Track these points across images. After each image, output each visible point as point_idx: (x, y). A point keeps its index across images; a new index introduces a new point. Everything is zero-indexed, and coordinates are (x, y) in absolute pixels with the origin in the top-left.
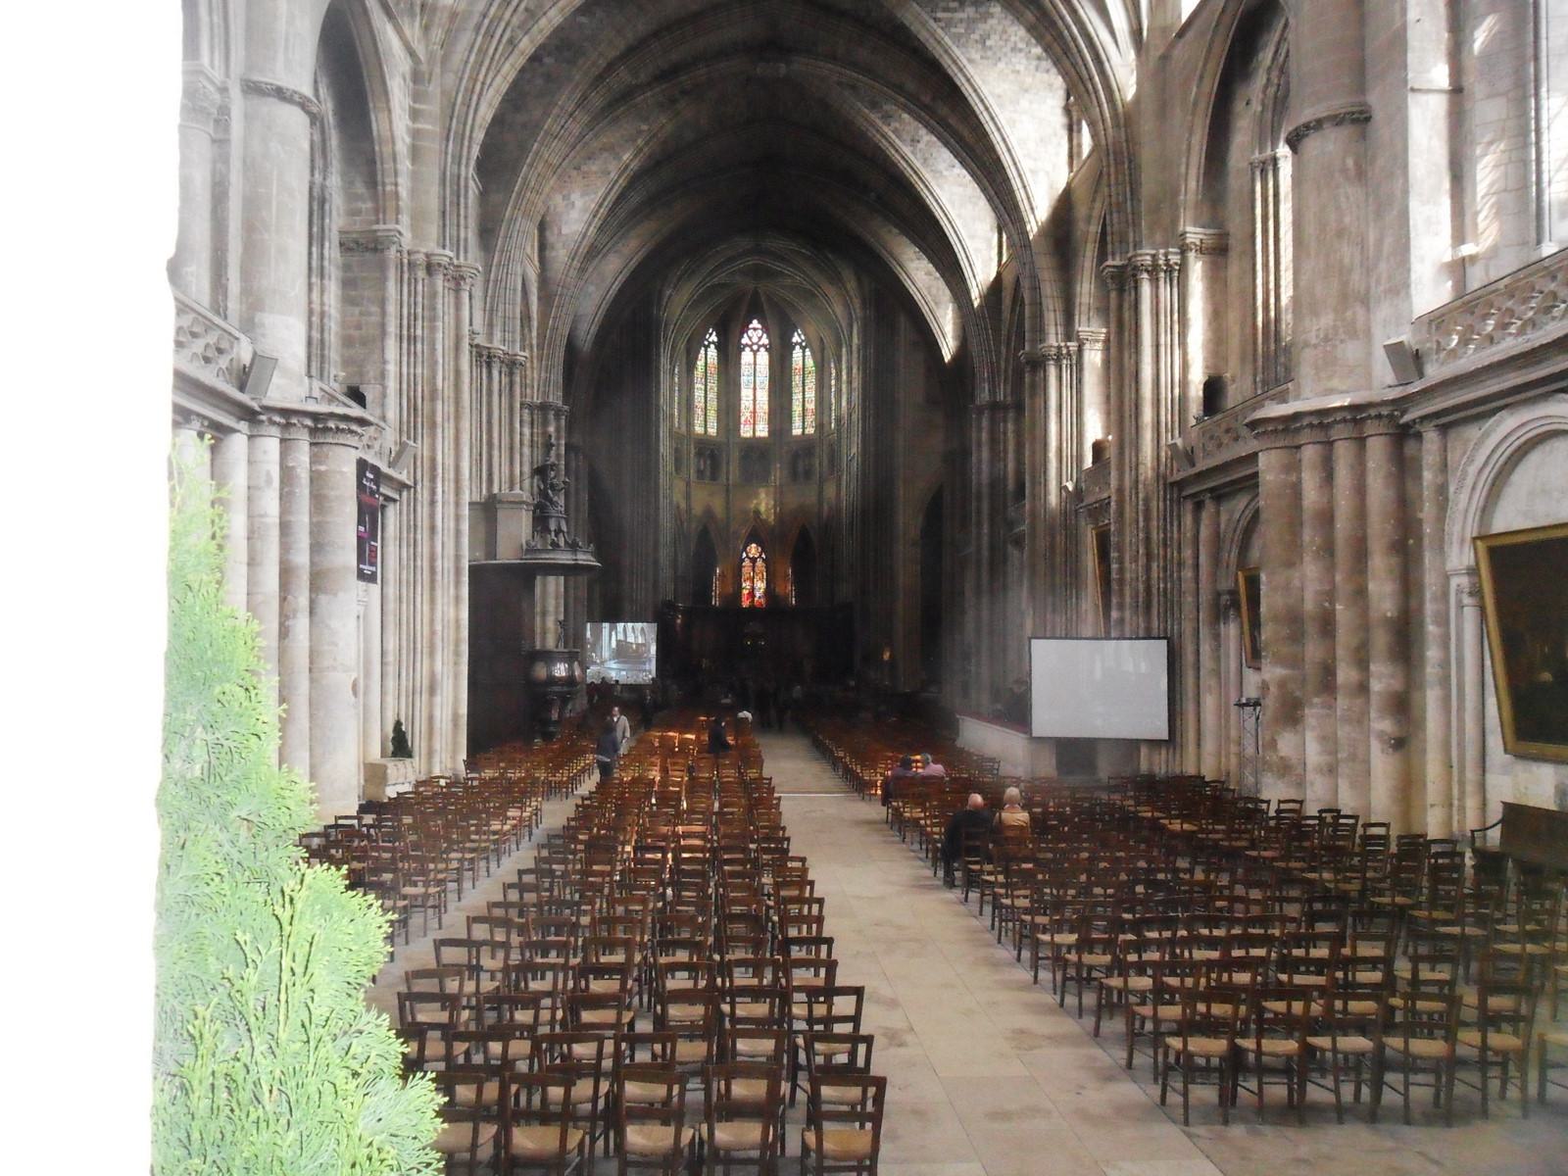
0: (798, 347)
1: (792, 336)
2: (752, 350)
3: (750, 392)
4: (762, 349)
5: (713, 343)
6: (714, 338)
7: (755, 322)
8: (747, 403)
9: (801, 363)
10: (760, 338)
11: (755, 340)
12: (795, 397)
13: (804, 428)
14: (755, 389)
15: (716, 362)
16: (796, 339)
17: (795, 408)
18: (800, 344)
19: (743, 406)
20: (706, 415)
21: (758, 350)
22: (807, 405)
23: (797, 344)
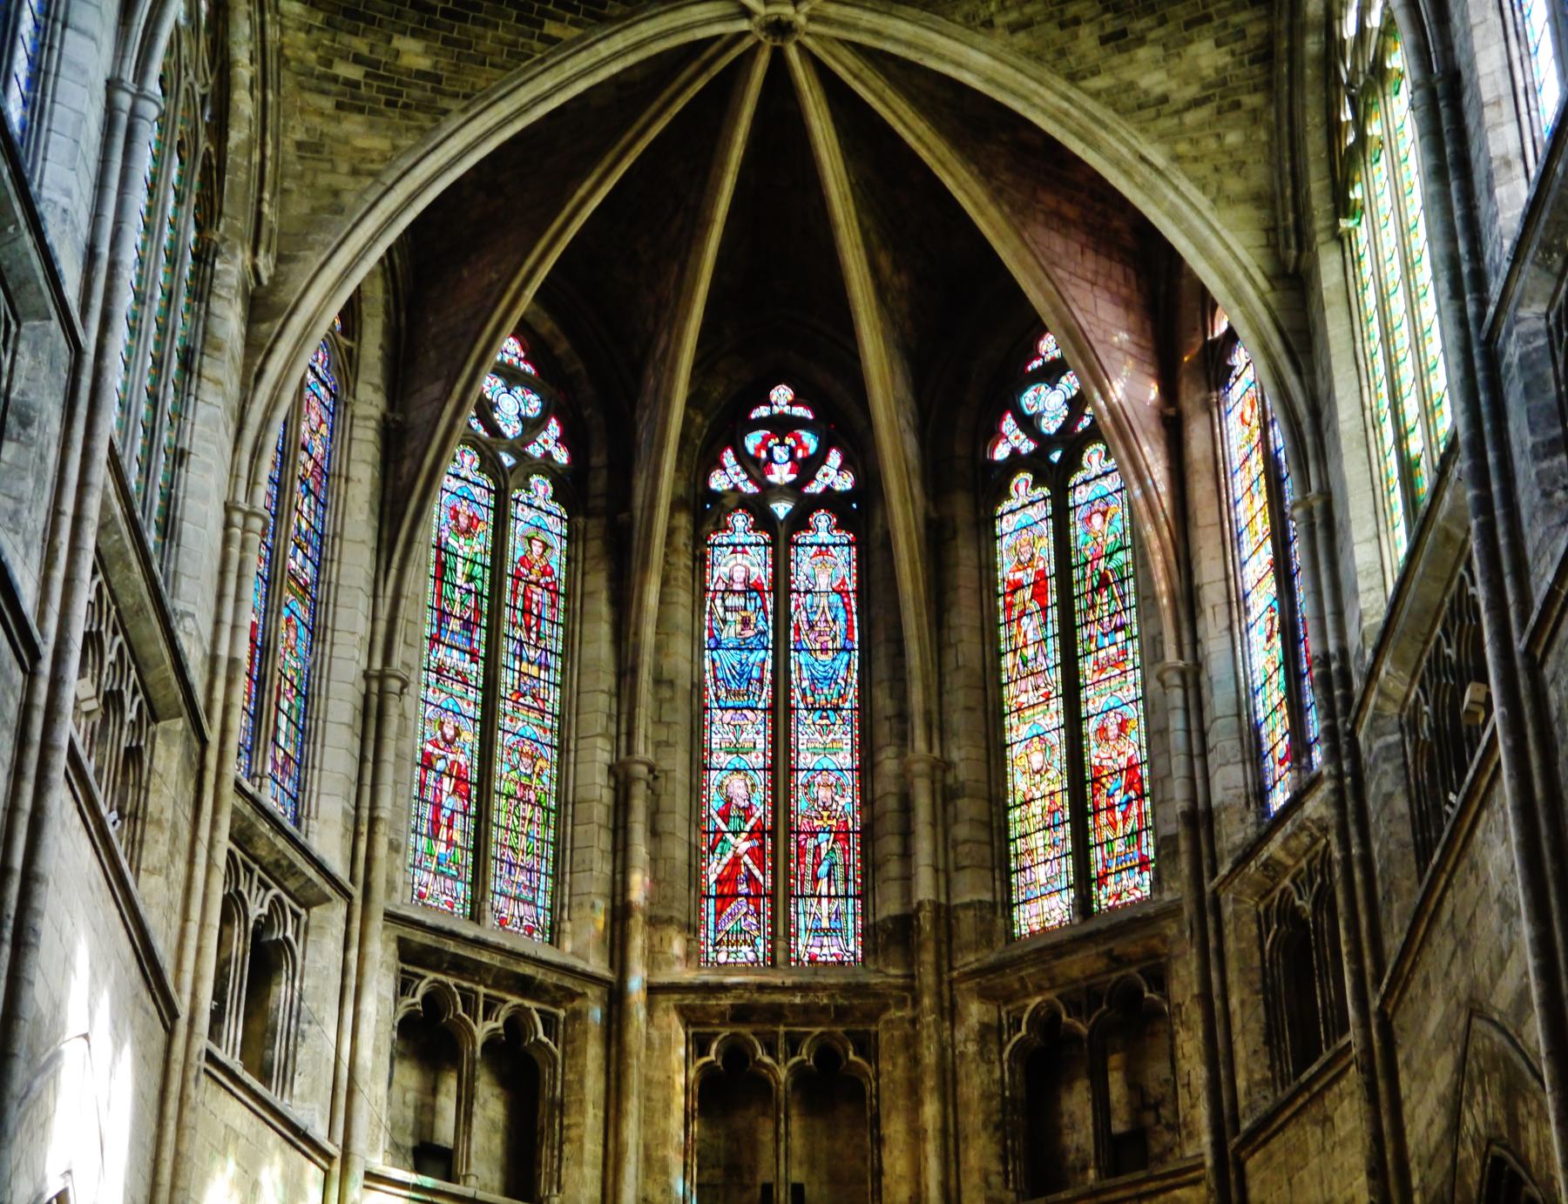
0: (1023, 478)
1: (996, 435)
2: (763, 520)
3: (755, 733)
4: (822, 519)
5: (546, 465)
6: (550, 443)
7: (782, 395)
8: (737, 787)
9: (1045, 548)
10: (807, 468)
11: (781, 474)
12: (1017, 730)
13: (1084, 882)
14: (780, 716)
15: (556, 560)
16: (1012, 440)
17: (1020, 783)
18: (1036, 465)
19: (717, 803)
20: (482, 820)
21: (800, 521)
22: (1095, 753)
23: (1016, 461)
